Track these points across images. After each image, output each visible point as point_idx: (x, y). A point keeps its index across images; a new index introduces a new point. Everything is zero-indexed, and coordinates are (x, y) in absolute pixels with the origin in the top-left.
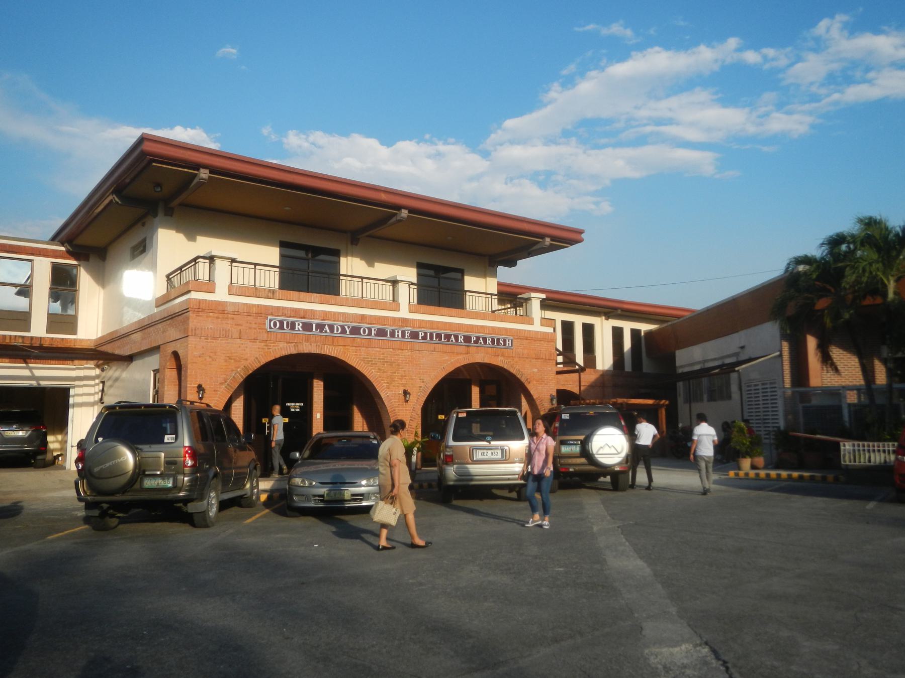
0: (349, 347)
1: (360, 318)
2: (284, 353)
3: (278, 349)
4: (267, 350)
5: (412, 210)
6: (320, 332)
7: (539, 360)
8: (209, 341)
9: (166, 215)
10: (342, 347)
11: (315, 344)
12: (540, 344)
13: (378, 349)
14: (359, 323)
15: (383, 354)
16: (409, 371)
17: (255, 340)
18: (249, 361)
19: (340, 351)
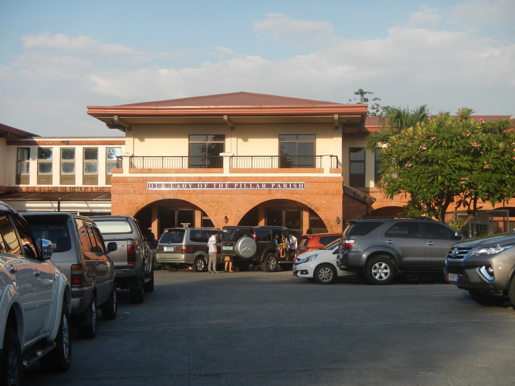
1: (198, 179)
2: (156, 200)
3: (153, 198)
4: (148, 198)
7: (327, 195)
9: (128, 131)
10: (188, 195)
12: (328, 185)
13: (210, 195)
14: (198, 182)
16: (229, 206)
17: (141, 194)
19: (187, 197)
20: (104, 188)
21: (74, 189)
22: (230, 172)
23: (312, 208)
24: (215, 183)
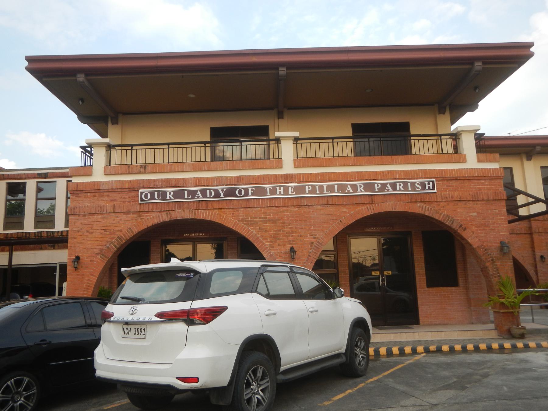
0: (225, 210)
2: (156, 221)
4: (140, 220)
6: (192, 198)
8: (86, 217)
9: (113, 124)
11: (189, 210)
12: (478, 183)
13: (259, 209)
14: (235, 185)
15: (265, 213)
17: (128, 213)
18: (123, 232)
21: (53, 234)
22: (296, 166)
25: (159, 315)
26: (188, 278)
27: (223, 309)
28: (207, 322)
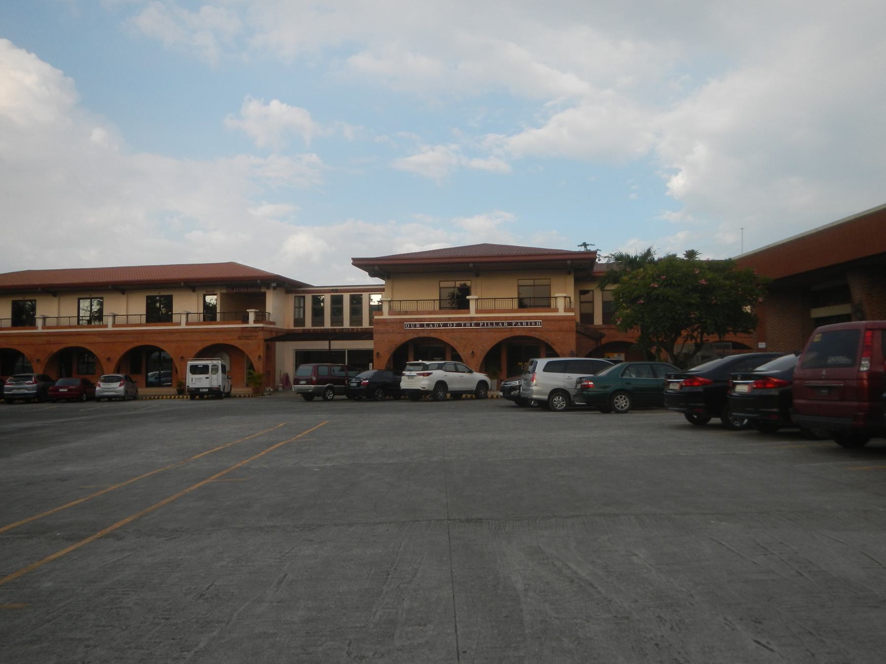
2: (411, 337)
5: (474, 263)
17: (399, 333)
20: (367, 328)
23: (549, 343)
24: (463, 323)
25: (417, 374)
26: (423, 366)
27: (432, 373)
28: (427, 376)
